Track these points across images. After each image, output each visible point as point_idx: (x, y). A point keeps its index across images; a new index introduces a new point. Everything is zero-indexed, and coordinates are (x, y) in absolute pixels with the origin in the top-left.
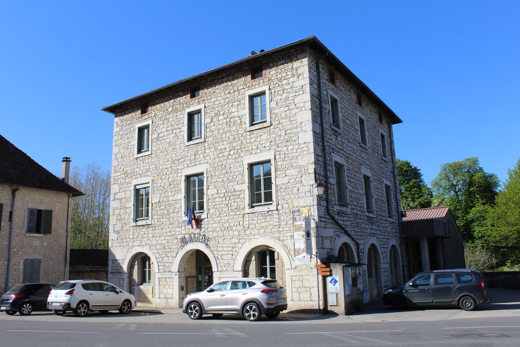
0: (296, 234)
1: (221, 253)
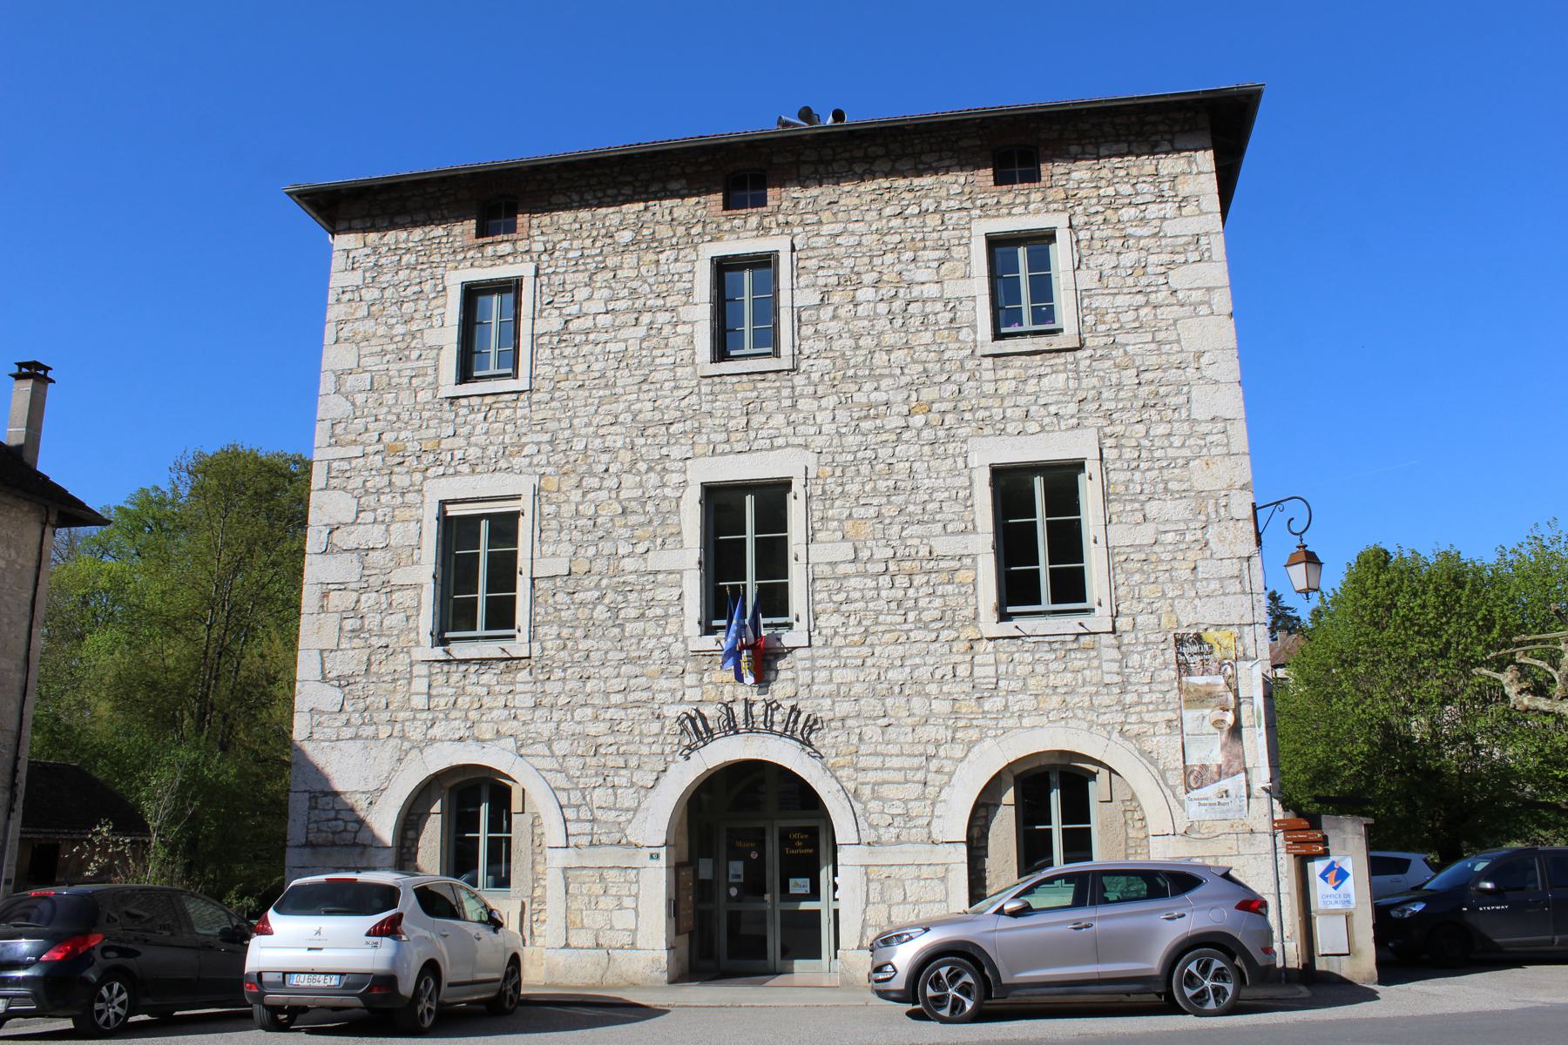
0: (1190, 715)
1: (872, 776)
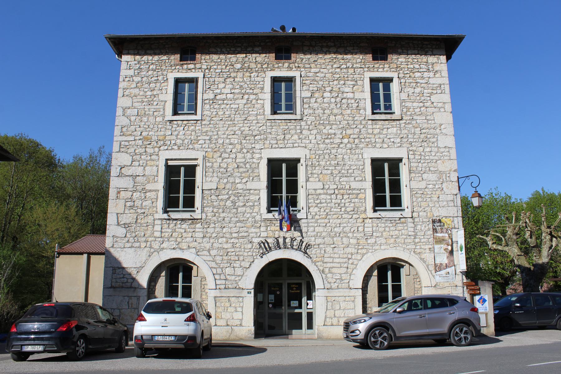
0: (437, 247)
1: (329, 265)
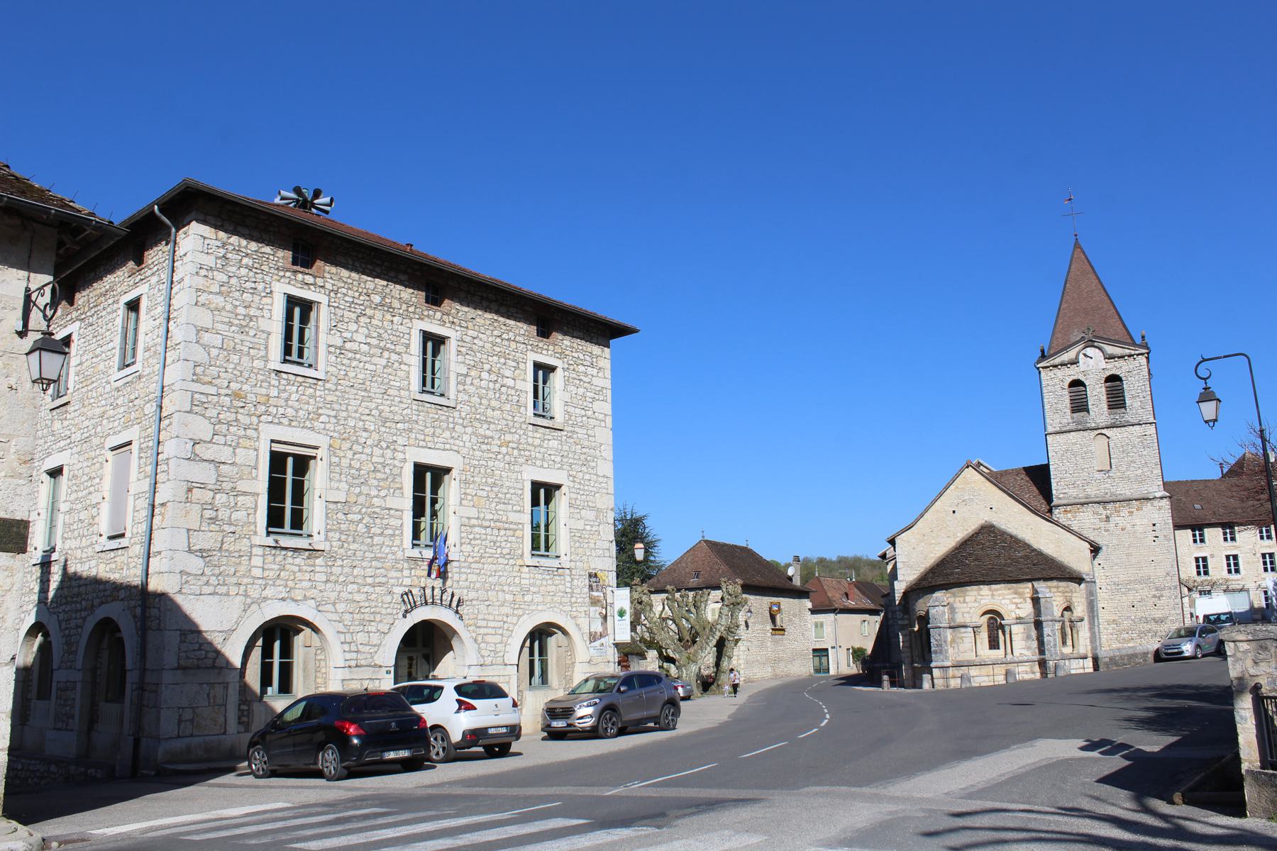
0: (592, 609)
1: (482, 631)
